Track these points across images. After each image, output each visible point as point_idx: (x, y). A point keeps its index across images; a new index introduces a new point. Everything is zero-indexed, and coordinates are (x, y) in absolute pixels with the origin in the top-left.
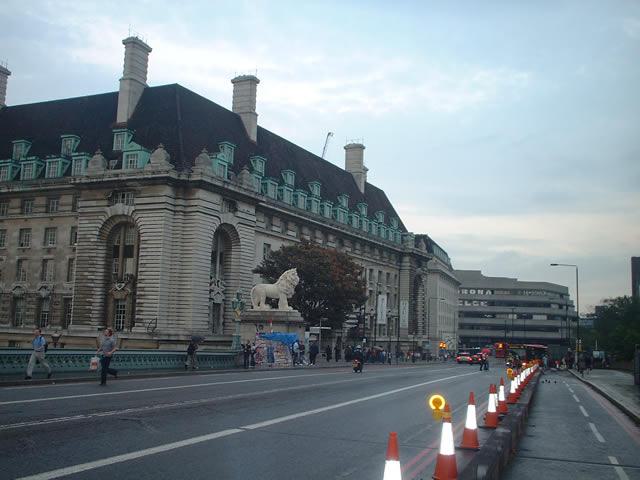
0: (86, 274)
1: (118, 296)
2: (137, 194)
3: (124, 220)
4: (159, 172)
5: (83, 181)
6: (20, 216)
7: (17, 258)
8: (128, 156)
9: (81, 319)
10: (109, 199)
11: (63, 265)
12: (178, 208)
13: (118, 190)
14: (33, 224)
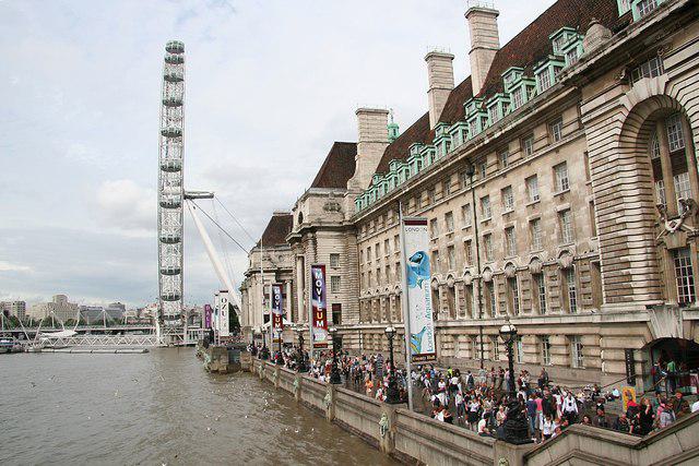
0: (613, 216)
3: (655, 107)
9: (618, 292)
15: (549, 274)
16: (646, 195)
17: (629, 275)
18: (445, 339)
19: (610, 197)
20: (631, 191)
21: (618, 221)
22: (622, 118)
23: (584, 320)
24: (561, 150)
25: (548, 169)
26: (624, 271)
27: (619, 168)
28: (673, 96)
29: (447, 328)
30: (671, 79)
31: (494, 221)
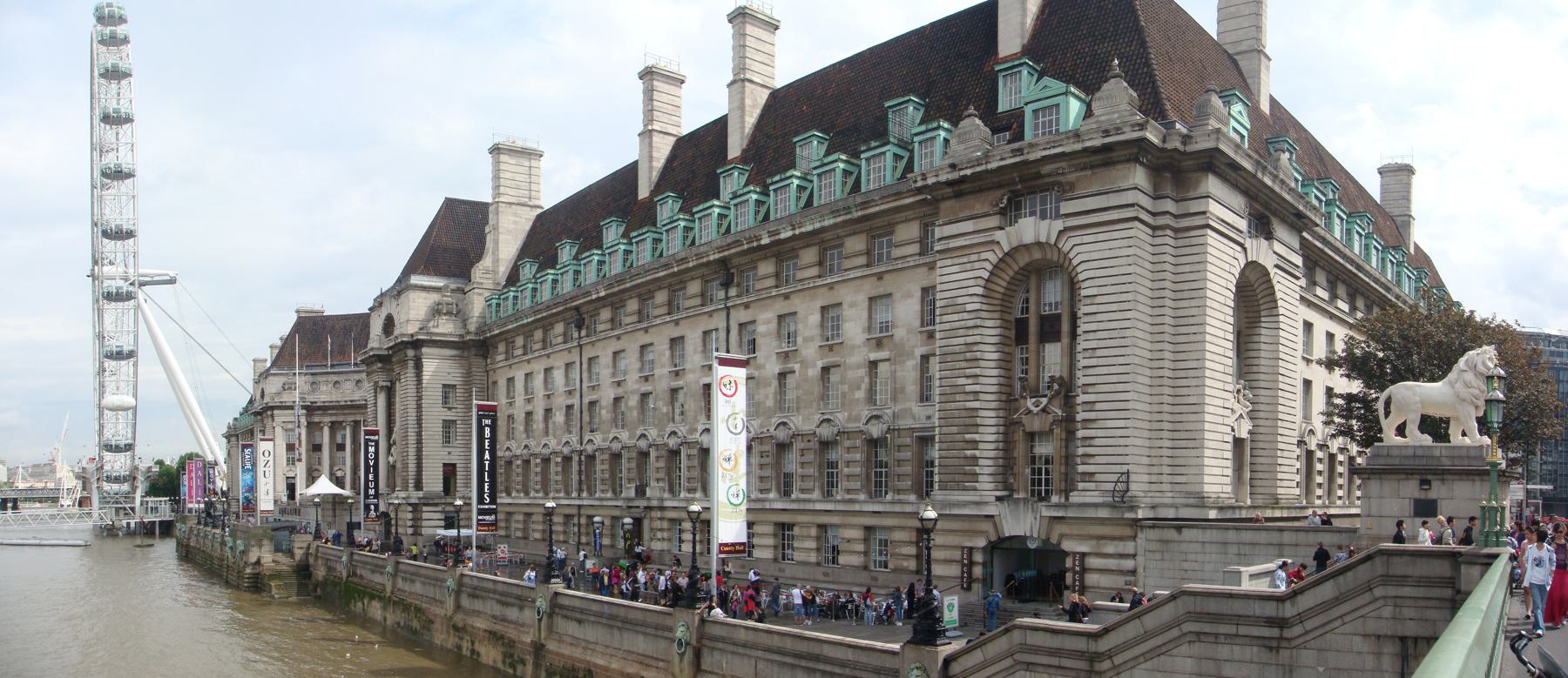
0: (962, 381)
1: (1035, 425)
2: (1066, 191)
3: (1037, 255)
4: (1118, 131)
5: (943, 178)
6: (819, 282)
7: (820, 364)
8: (1035, 112)
9: (957, 478)
10: (1002, 212)
11: (909, 372)
12: (1162, 221)
13: (1020, 187)
14: (845, 294)
15: (847, 443)
16: (1005, 363)
17: (975, 458)
18: (658, 524)
19: (961, 357)
20: (991, 354)
21: (968, 388)
22: (993, 258)
23: (898, 508)
24: (887, 277)
25: (862, 299)
26: (969, 453)
27: (979, 322)
28: (1066, 249)
29: (662, 509)
30: (1066, 229)
31: (761, 360)
